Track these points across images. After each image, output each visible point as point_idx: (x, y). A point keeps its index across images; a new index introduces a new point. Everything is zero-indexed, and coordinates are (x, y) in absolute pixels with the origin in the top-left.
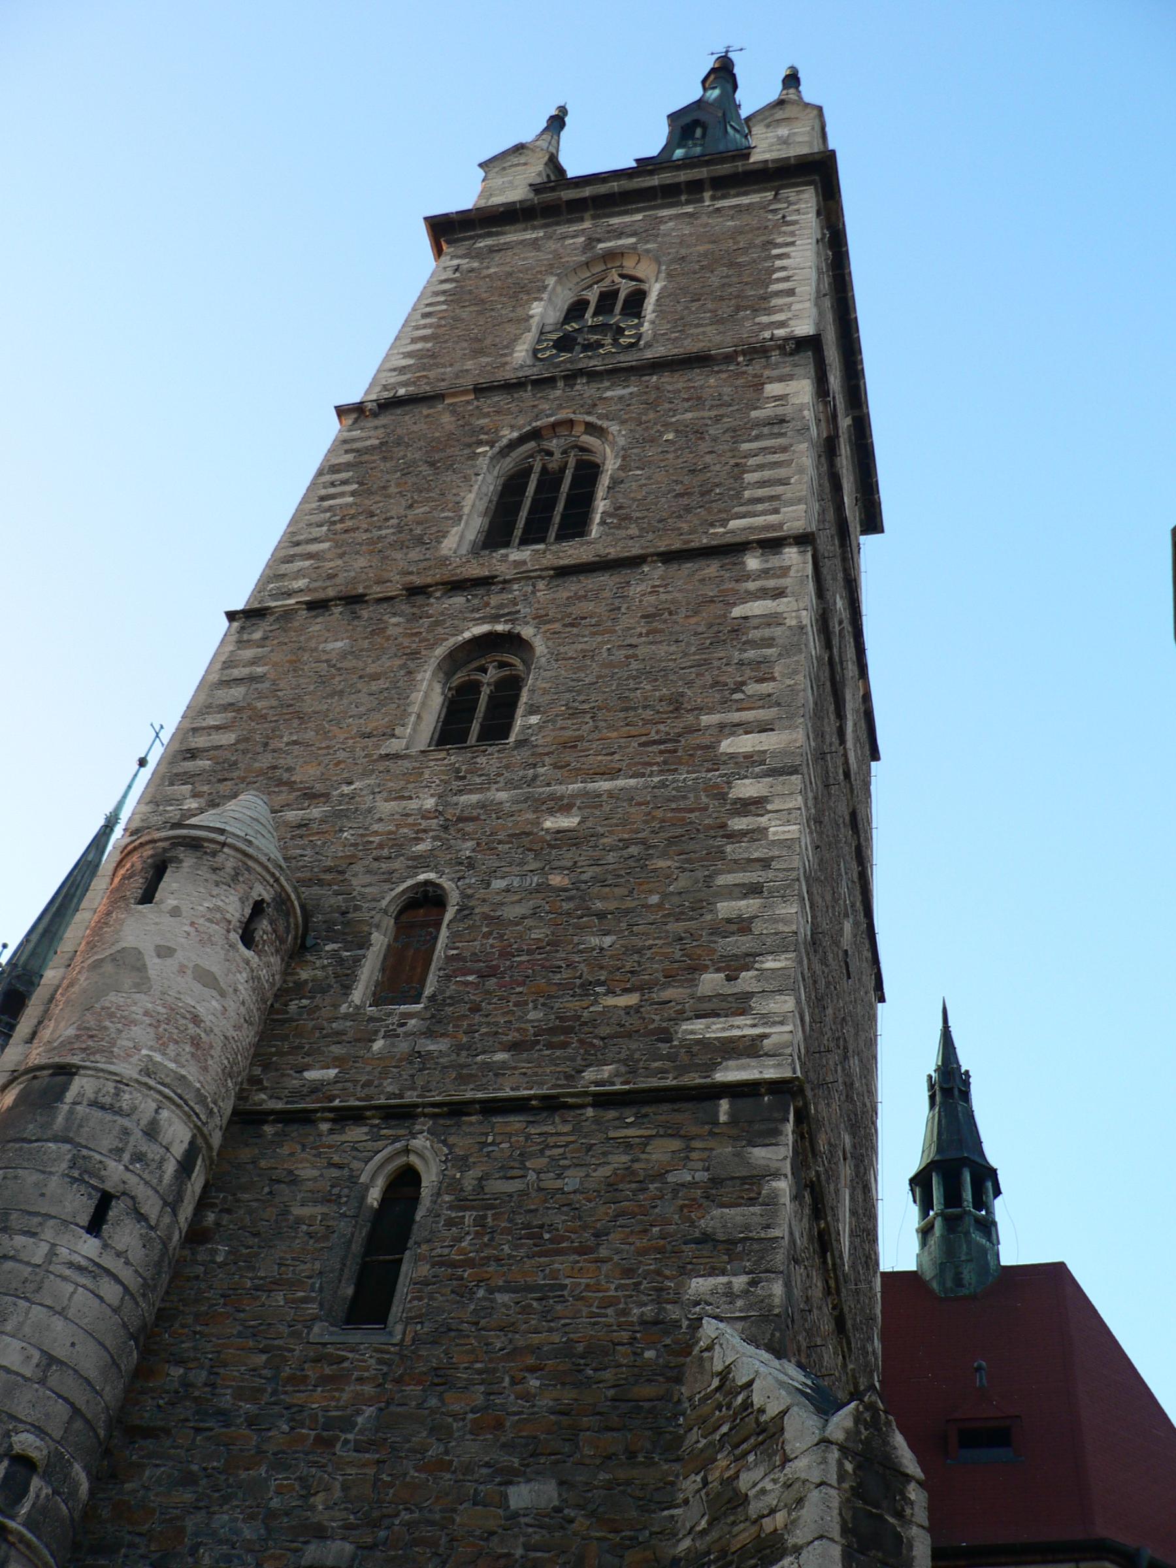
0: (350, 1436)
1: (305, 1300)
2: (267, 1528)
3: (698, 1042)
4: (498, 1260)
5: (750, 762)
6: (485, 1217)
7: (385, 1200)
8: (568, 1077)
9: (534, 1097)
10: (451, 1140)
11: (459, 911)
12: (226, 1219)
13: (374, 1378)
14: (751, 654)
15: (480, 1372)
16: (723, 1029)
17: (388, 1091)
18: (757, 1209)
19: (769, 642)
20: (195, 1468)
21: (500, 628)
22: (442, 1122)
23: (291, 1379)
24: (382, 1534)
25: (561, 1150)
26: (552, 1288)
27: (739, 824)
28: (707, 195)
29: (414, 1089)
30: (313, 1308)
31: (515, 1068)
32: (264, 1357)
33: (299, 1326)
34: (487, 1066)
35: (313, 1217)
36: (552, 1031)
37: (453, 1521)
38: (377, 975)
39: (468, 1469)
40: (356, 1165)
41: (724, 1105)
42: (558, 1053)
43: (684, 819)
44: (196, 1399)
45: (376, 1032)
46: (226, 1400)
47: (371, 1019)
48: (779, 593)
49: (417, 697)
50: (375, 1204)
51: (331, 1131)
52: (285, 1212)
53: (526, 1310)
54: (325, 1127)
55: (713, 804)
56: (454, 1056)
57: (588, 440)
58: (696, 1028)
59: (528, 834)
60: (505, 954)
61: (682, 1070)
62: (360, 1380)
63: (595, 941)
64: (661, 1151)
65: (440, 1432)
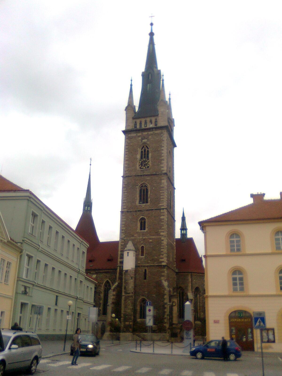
5: (162, 235)
14: (162, 223)
19: (163, 222)
21: (143, 217)
27: (162, 242)
28: (154, 130)
48: (164, 216)
49: (138, 225)
57: (146, 185)
64: (159, 269)
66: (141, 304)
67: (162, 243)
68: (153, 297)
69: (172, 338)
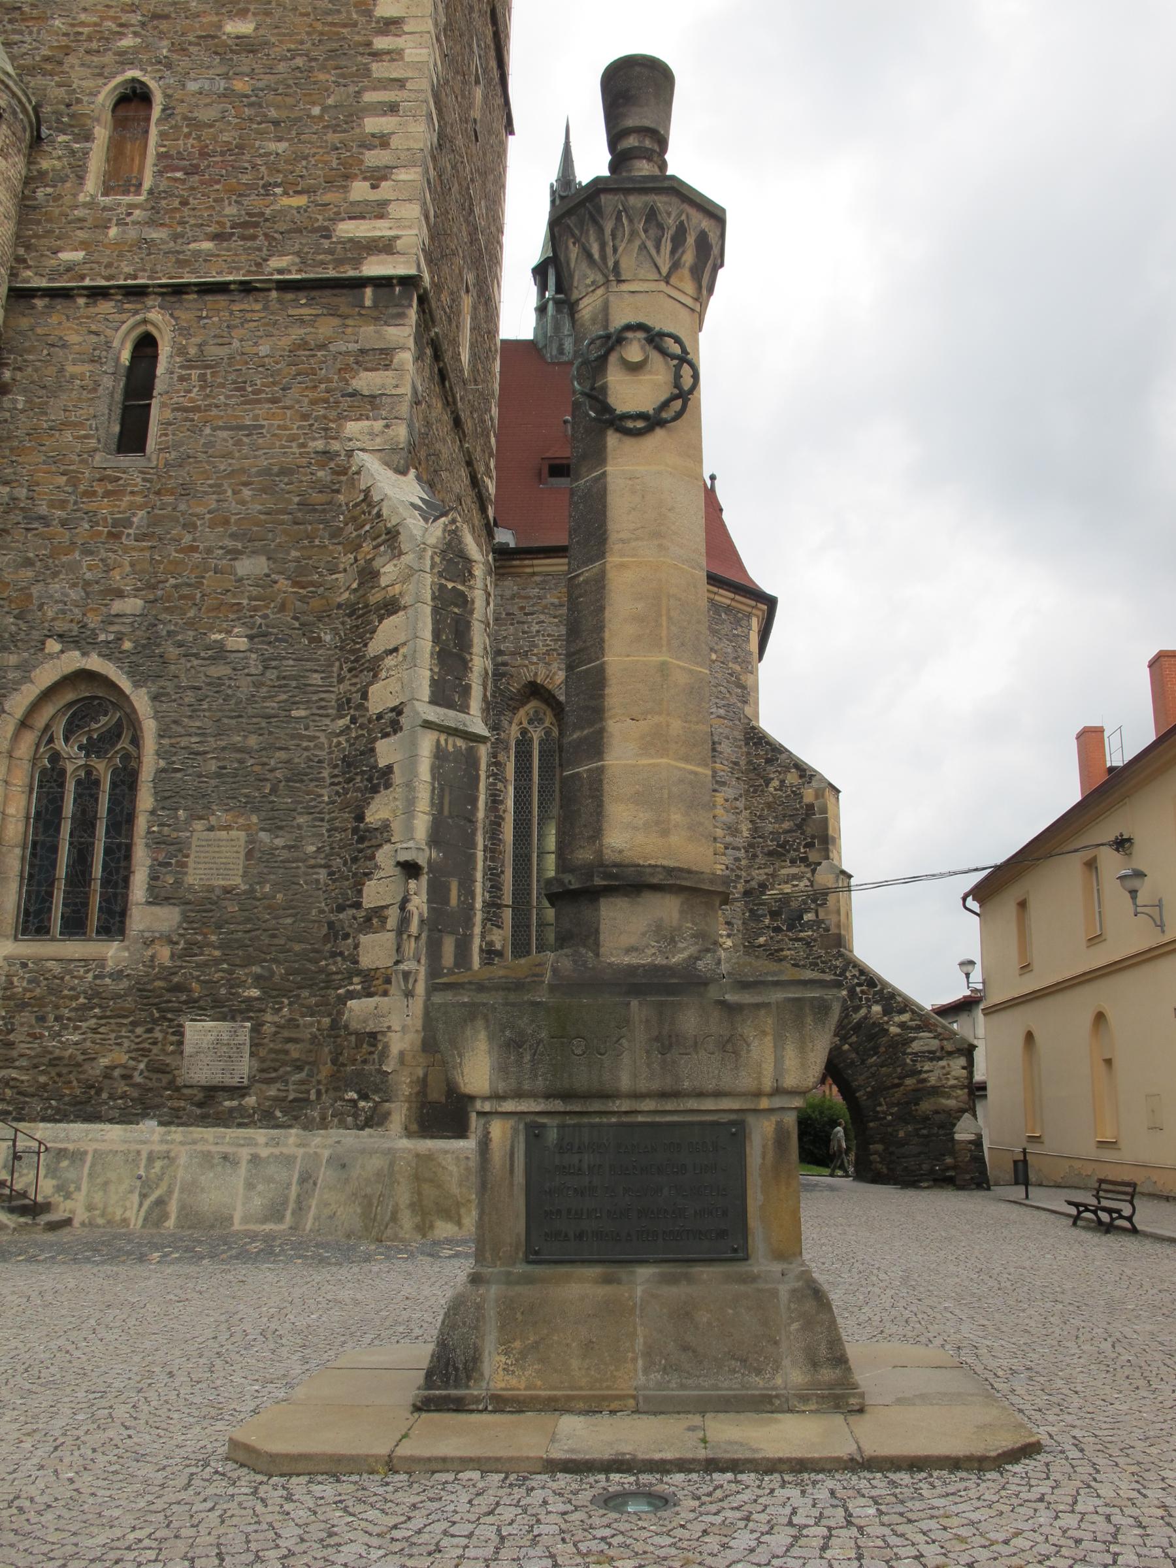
0: (131, 531)
1: (86, 437)
2: (85, 592)
3: (351, 240)
4: (217, 406)
6: (205, 375)
7: (134, 357)
8: (258, 265)
9: (234, 282)
10: (177, 313)
11: (163, 110)
12: (19, 375)
13: (141, 492)
15: (210, 486)
16: (369, 230)
17: (126, 273)
18: (389, 373)
20: (31, 555)
22: (168, 298)
23: (86, 494)
24: (159, 593)
25: (255, 324)
26: (256, 427)
27: (381, 43)
29: (145, 270)
30: (93, 442)
31: (218, 256)
32: (65, 478)
33: (85, 456)
34: (197, 253)
35: (83, 374)
36: (245, 225)
37: (202, 584)
38: (103, 166)
39: (209, 551)
40: (109, 332)
41: (369, 292)
42: (249, 244)
43: (338, 33)
44: (22, 509)
45: (110, 220)
46: (43, 509)
47: (104, 209)
50: (127, 363)
51: (87, 305)
52: (62, 370)
53: (238, 443)
54: (81, 301)
55: (363, 20)
56: (172, 244)
58: (348, 229)
59: (213, 37)
60: (203, 154)
61: (339, 262)
62: (132, 493)
63: (272, 146)
64: (326, 328)
65: (190, 527)
66: (55, 757)
67: (377, 55)
68: (220, 653)
69: (580, 1288)
